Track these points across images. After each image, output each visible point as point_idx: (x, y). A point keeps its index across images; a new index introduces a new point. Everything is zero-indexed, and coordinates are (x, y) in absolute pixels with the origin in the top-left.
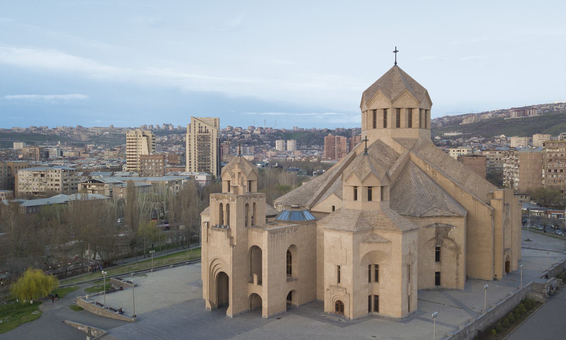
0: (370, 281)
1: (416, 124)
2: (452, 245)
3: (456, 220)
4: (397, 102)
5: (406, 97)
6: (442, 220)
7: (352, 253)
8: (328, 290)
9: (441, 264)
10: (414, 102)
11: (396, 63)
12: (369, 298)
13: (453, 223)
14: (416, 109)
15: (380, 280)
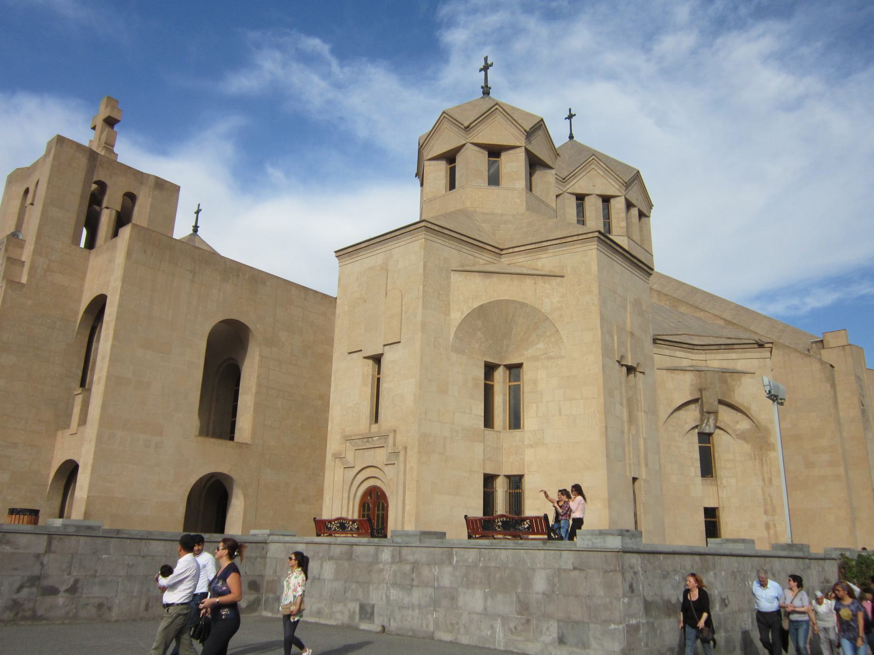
0: (488, 422)
1: (620, 227)
2: (744, 425)
3: (749, 355)
4: (576, 180)
5: (595, 172)
6: (708, 357)
7: (421, 295)
8: (338, 456)
9: (719, 483)
10: (613, 183)
11: (571, 137)
12: (485, 486)
13: (740, 365)
14: (618, 199)
15: (526, 417)
